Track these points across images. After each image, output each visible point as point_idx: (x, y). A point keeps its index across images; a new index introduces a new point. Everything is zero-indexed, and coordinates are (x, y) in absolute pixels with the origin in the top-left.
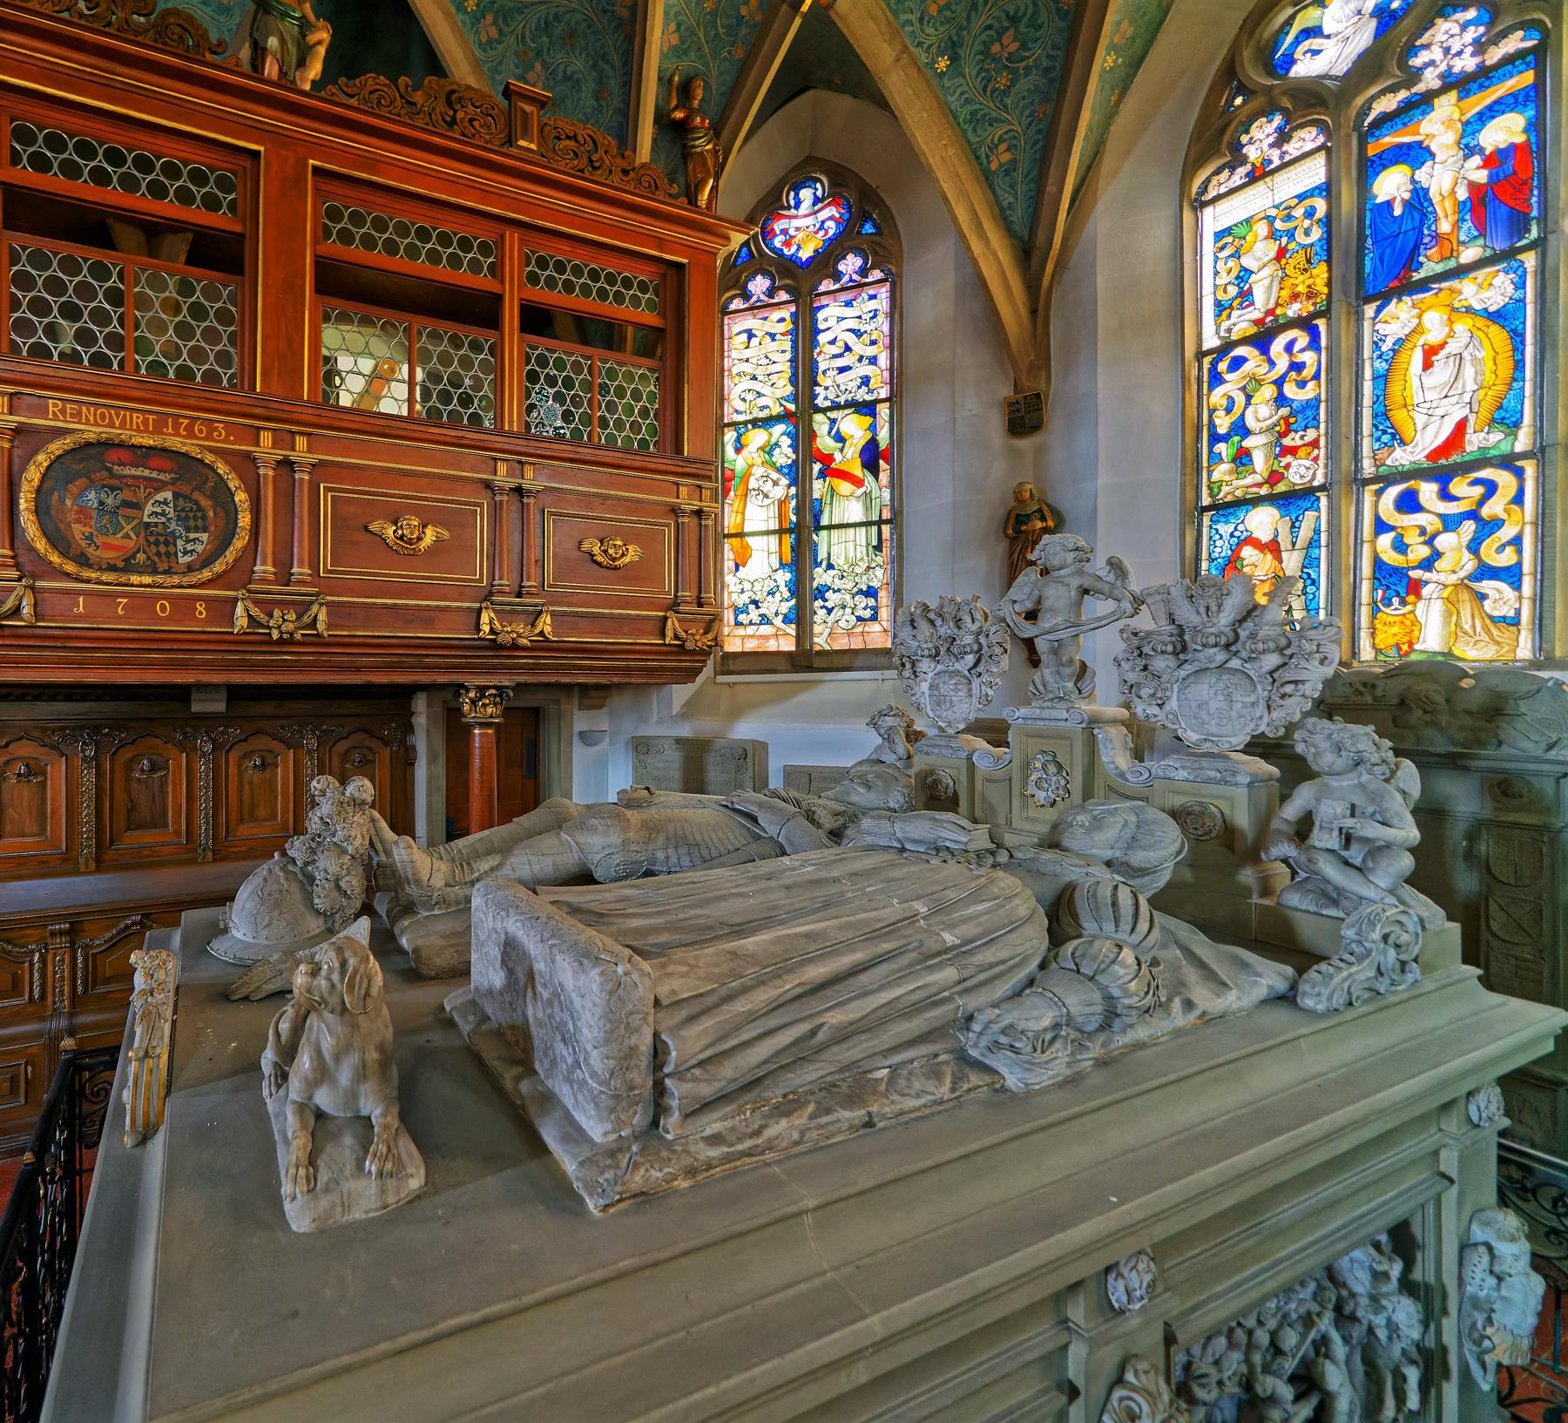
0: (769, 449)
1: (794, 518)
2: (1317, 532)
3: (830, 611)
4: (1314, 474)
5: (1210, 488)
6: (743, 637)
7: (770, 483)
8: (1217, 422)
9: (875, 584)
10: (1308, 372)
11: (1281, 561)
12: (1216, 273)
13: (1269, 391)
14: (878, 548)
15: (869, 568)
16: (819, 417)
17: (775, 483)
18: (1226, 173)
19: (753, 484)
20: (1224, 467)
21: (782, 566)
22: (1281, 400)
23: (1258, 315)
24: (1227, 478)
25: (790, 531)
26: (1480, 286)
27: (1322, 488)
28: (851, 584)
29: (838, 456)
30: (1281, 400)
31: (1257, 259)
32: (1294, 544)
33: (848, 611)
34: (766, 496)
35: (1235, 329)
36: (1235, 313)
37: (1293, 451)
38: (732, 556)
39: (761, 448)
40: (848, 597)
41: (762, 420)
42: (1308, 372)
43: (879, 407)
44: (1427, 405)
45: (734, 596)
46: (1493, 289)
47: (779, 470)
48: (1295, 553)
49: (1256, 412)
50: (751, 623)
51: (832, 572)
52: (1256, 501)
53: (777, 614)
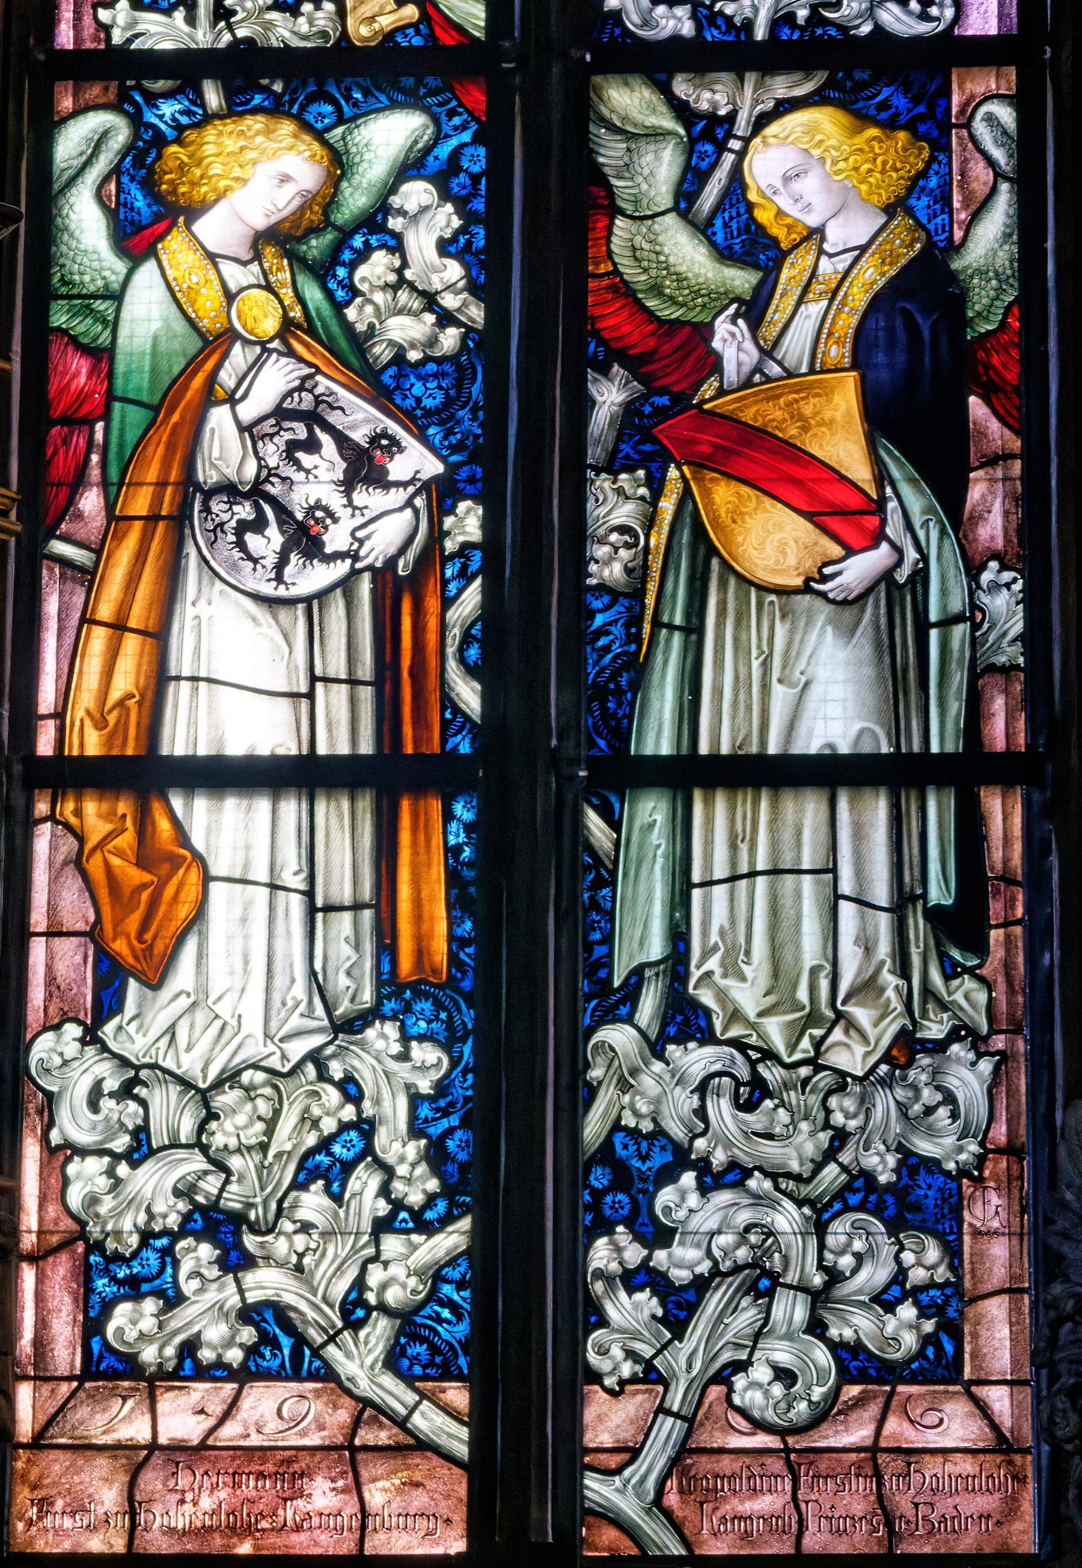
0: (319, 243)
1: (469, 695)
3: (679, 1306)
6: (136, 1459)
7: (327, 464)
9: (943, 1144)
14: (960, 928)
15: (907, 1047)
16: (628, 100)
17: (364, 467)
19: (223, 450)
21: (395, 994)
25: (438, 776)
28: (808, 1143)
29: (732, 344)
33: (792, 1310)
34: (305, 539)
38: (76, 910)
39: (279, 239)
40: (787, 1219)
41: (284, 61)
43: (968, 86)
45: (86, 1176)
47: (382, 383)
50: (189, 1365)
51: (697, 1060)
53: (355, 1311)
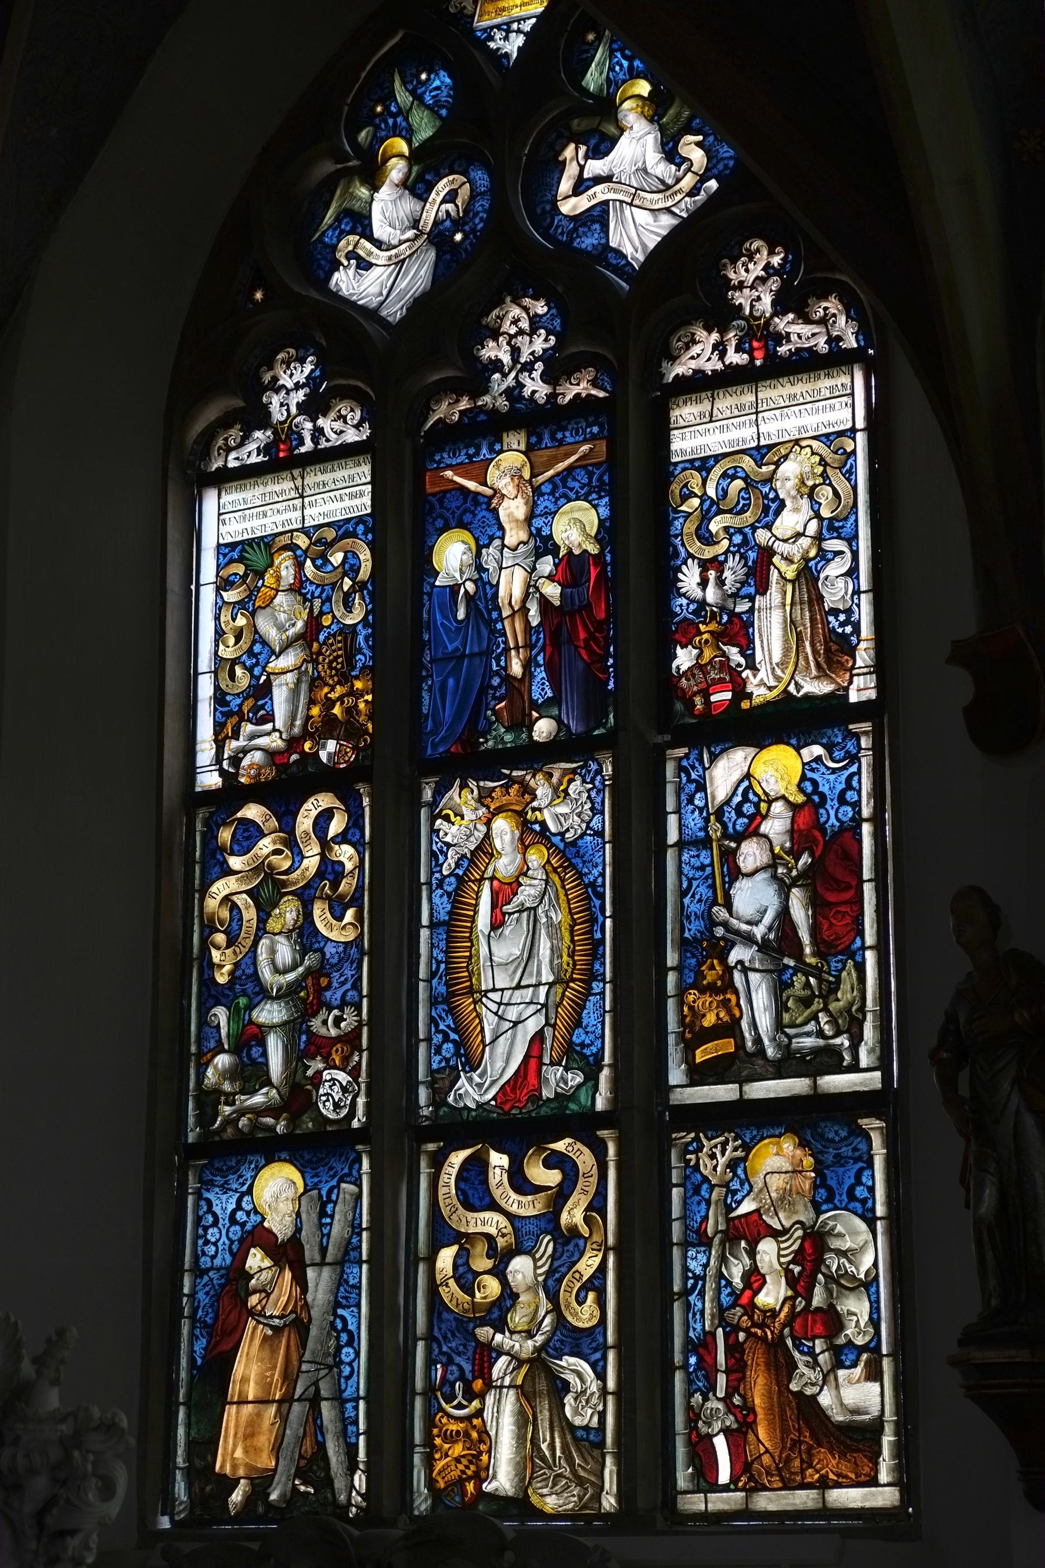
2: (356, 1228)
4: (353, 1104)
5: (198, 1105)
8: (216, 956)
10: (347, 886)
11: (304, 1290)
12: (219, 634)
13: (288, 912)
18: (235, 434)
20: (223, 1060)
22: (305, 935)
23: (274, 742)
24: (227, 1087)
26: (555, 790)
27: (363, 1135)
30: (305, 935)
31: (281, 628)
32: (323, 1250)
35: (245, 762)
36: (248, 728)
37: (320, 1047)
42: (347, 886)
44: (496, 996)
46: (567, 804)
48: (326, 1272)
49: (273, 951)
52: (269, 1149)
